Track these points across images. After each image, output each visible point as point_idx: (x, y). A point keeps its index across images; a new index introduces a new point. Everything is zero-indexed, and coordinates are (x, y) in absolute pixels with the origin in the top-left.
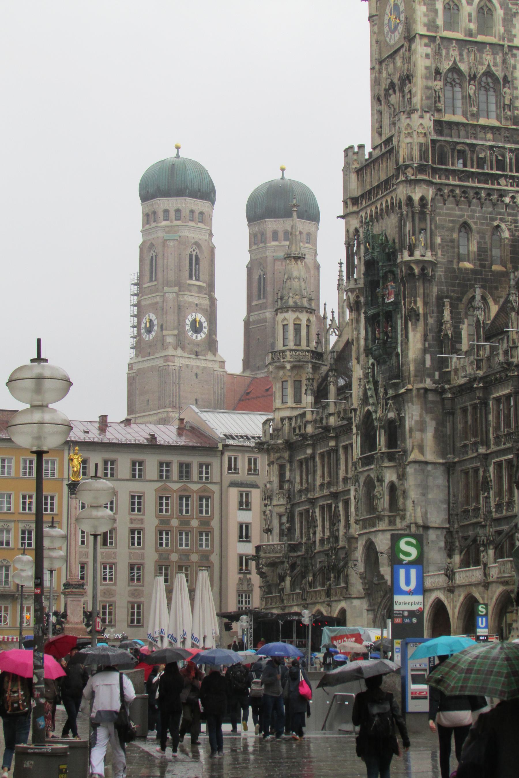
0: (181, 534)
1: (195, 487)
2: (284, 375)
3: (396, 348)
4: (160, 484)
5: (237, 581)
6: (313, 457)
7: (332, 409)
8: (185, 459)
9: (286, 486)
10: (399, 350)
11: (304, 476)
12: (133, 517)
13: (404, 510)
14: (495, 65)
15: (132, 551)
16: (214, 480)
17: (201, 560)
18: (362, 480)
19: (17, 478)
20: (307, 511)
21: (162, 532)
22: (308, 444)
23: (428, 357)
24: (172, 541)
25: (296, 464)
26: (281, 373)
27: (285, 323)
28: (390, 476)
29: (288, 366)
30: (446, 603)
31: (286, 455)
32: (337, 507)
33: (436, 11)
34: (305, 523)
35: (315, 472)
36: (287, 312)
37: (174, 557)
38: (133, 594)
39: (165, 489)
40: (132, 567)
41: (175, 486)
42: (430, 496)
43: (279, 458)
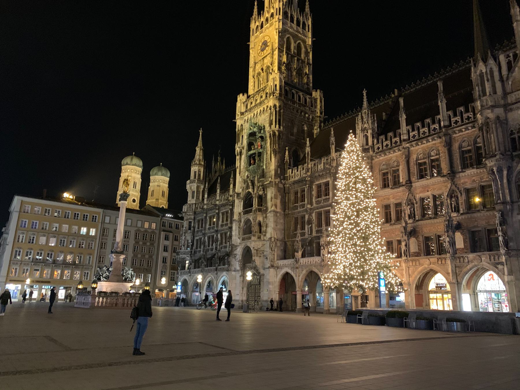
3: (263, 166)
6: (206, 217)
7: (218, 198)
9: (192, 229)
10: (264, 167)
11: (200, 225)
13: (266, 232)
14: (303, 67)
18: (243, 220)
20: (201, 239)
23: (279, 169)
28: (260, 218)
30: (292, 274)
32: (217, 235)
33: (284, 41)
34: (199, 243)
35: (206, 223)
42: (278, 227)
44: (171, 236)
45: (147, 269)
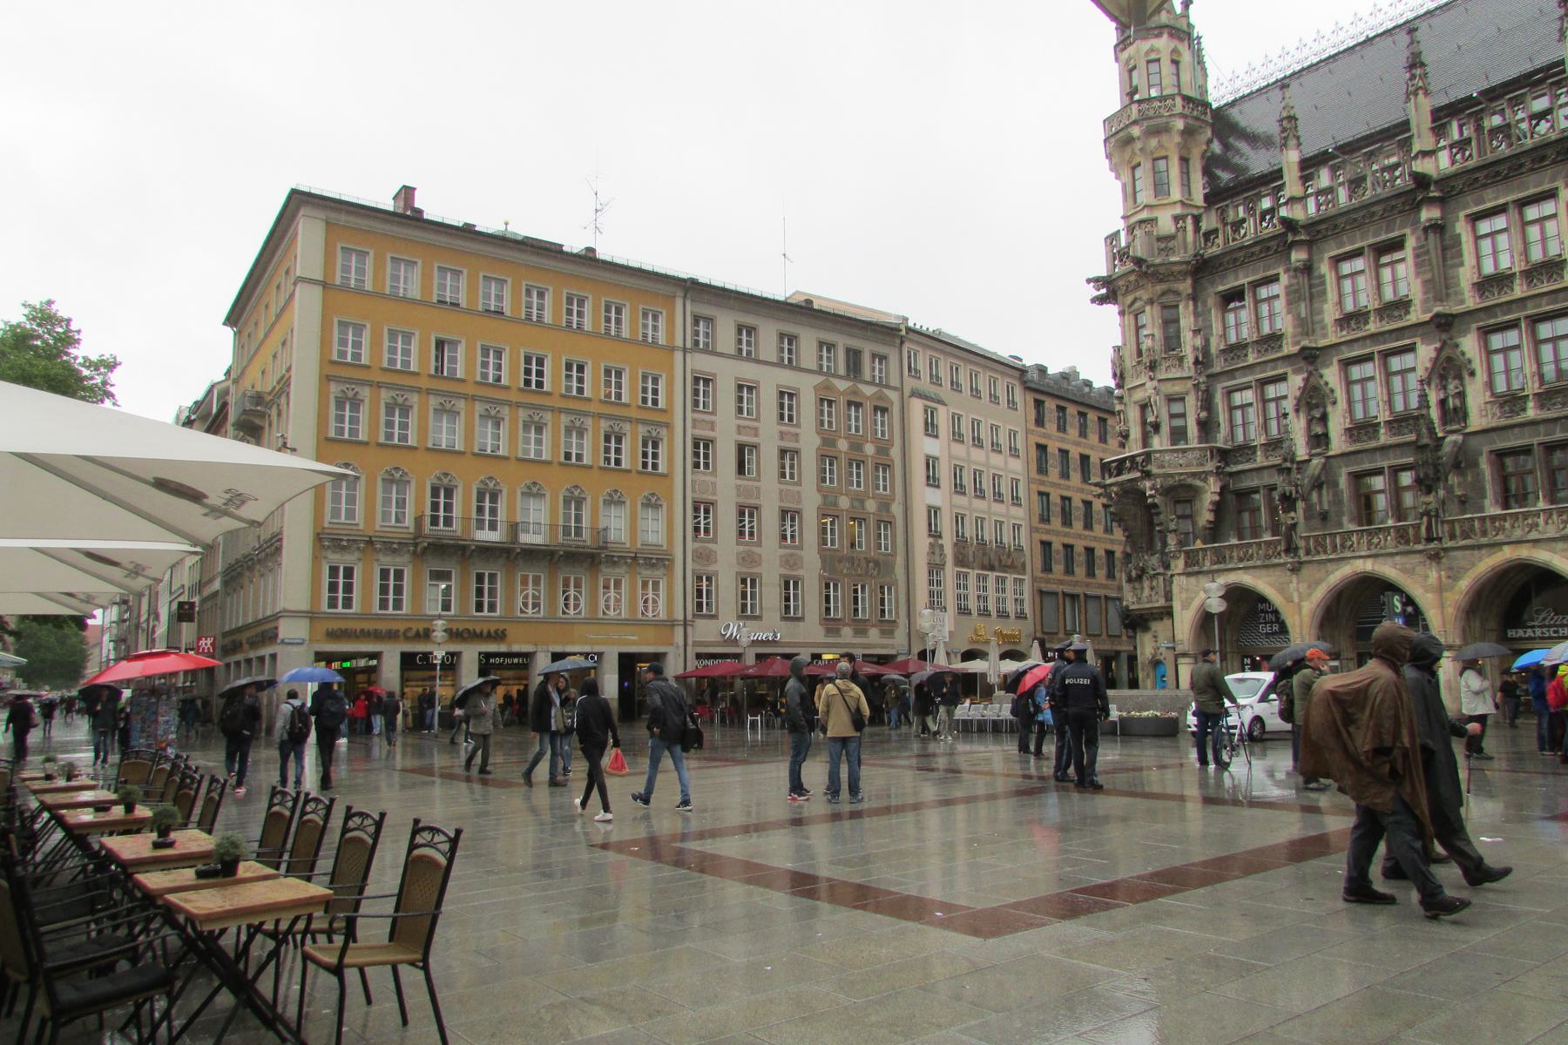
0: (851, 465)
1: (868, 391)
2: (1160, 146)
4: (822, 378)
5: (926, 549)
8: (856, 343)
12: (784, 429)
15: (784, 487)
16: (893, 383)
17: (879, 510)
19: (594, 335)
21: (827, 456)
22: (1301, 243)
24: (839, 476)
25: (1211, 301)
26: (1153, 142)
27: (1153, 56)
29: (1179, 124)
31: (1186, 286)
36: (1159, 36)
37: (844, 503)
38: (787, 562)
39: (828, 387)
40: (784, 513)
41: (842, 385)
43: (1163, 294)
44: (943, 418)
45: (877, 563)
